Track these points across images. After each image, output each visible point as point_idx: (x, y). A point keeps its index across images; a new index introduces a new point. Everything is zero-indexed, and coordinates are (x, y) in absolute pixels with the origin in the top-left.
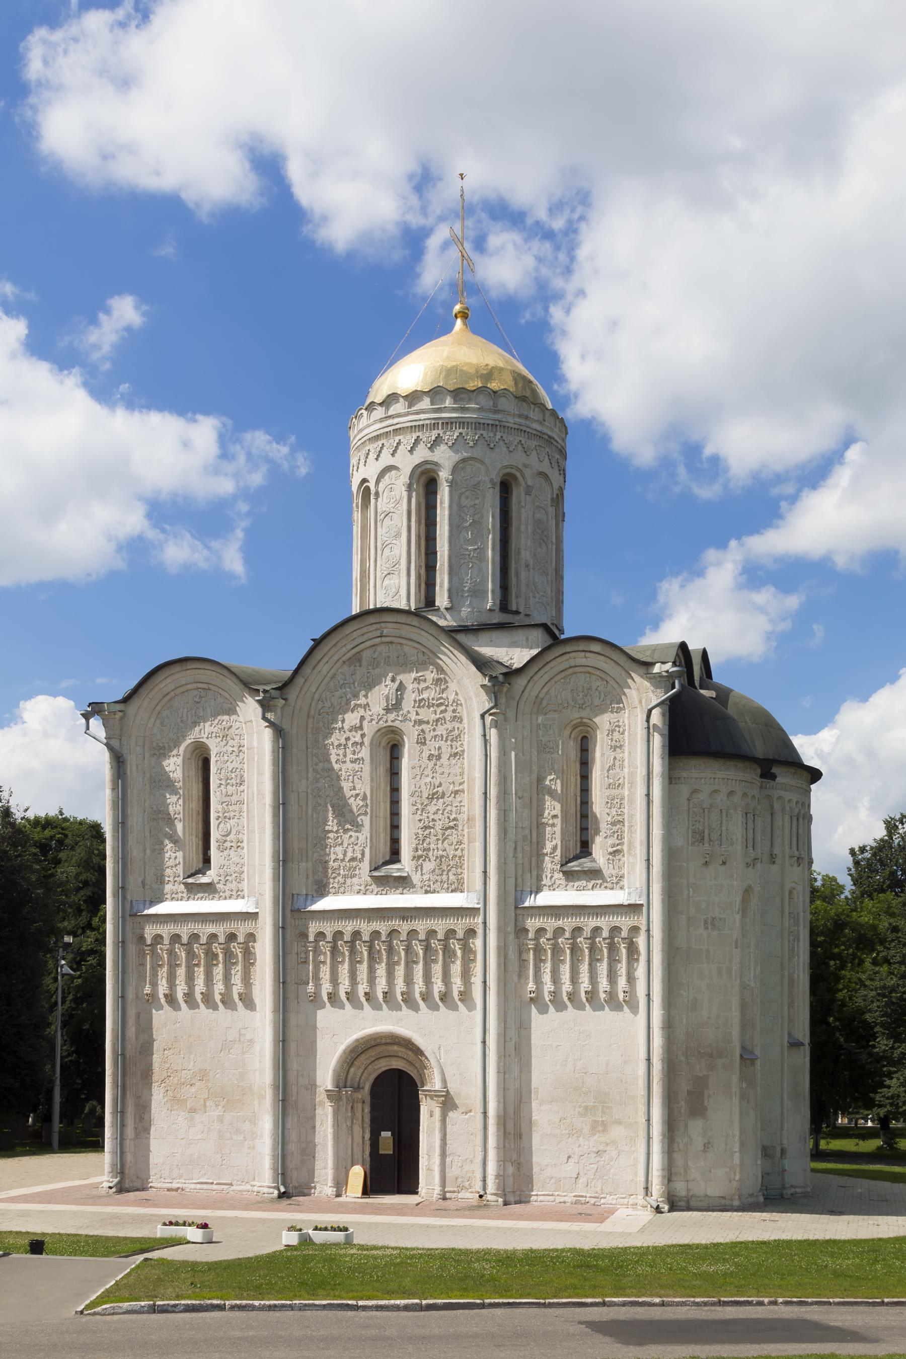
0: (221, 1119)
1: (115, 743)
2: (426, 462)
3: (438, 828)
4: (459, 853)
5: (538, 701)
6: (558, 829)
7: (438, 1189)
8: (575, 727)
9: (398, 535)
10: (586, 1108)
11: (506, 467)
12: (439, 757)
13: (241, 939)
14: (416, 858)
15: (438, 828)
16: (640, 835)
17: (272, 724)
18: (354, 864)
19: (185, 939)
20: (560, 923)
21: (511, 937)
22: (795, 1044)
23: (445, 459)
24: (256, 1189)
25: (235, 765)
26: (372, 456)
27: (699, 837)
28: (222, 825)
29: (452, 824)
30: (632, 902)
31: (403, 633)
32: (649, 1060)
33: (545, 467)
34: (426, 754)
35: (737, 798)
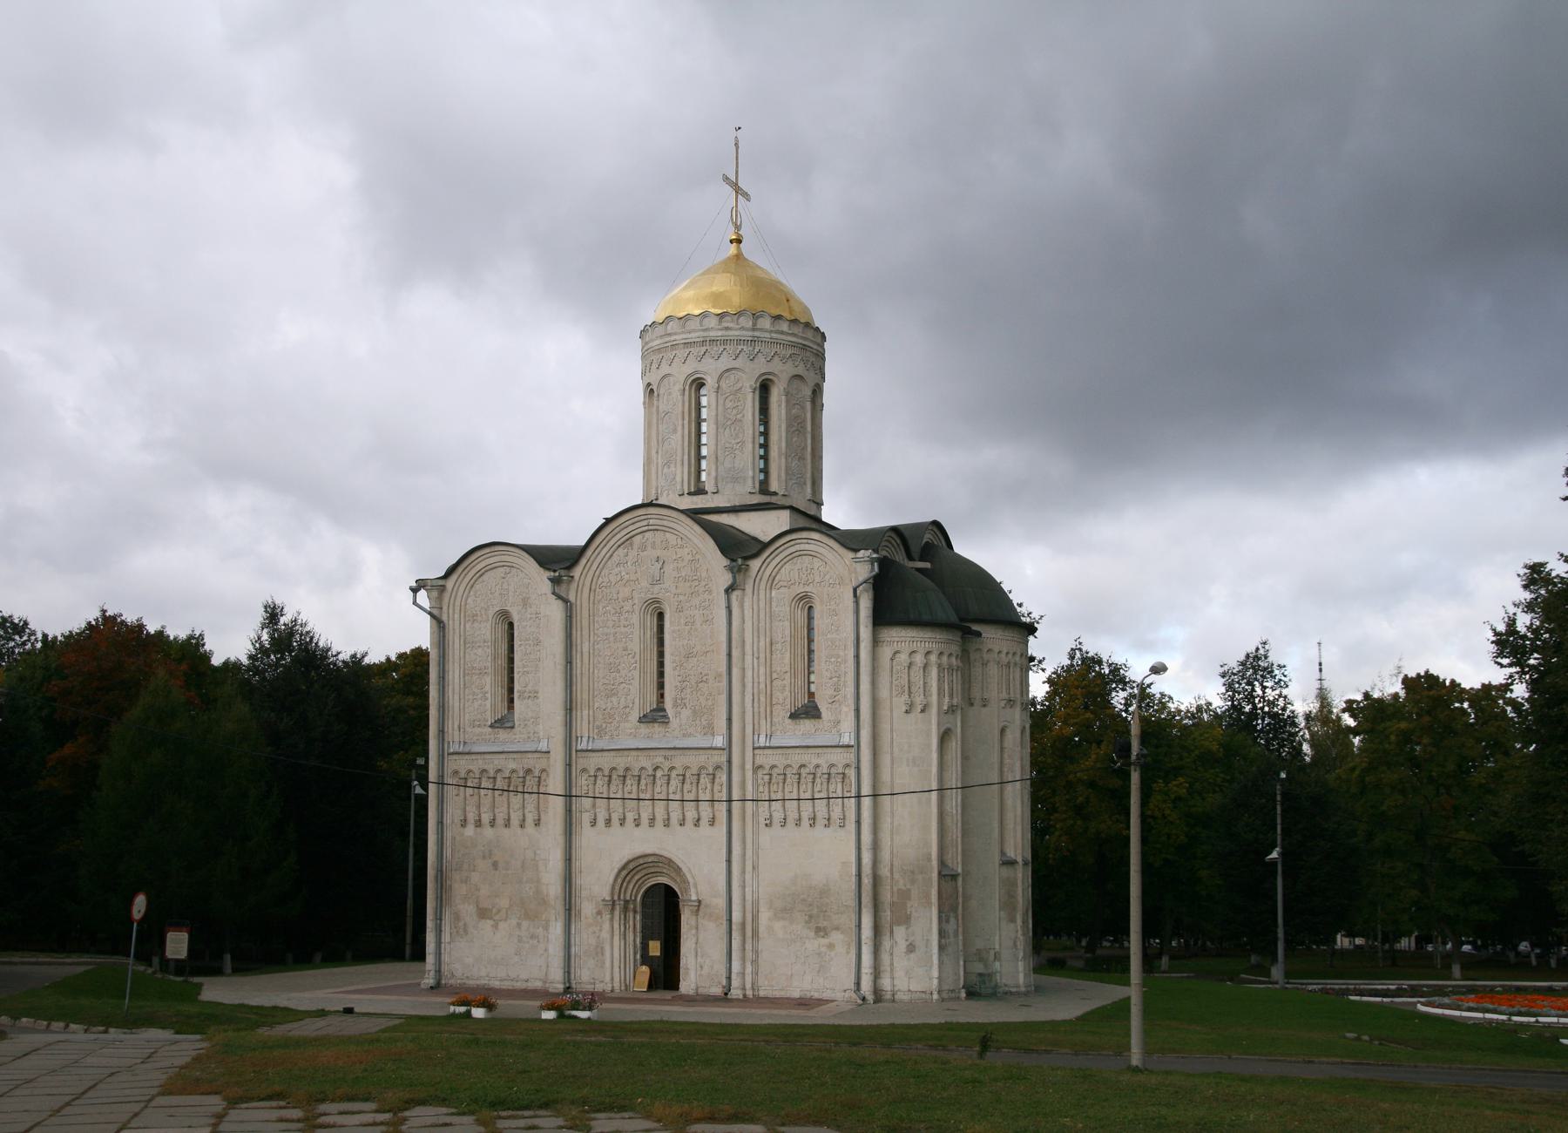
0: (519, 925)
1: (435, 612)
6: (787, 682)
7: (693, 986)
8: (801, 599)
9: (675, 431)
14: (675, 705)
16: (851, 690)
17: (559, 597)
21: (749, 774)
22: (1011, 863)
23: (710, 369)
26: (654, 366)
32: (859, 875)
33: (800, 370)
35: (933, 658)
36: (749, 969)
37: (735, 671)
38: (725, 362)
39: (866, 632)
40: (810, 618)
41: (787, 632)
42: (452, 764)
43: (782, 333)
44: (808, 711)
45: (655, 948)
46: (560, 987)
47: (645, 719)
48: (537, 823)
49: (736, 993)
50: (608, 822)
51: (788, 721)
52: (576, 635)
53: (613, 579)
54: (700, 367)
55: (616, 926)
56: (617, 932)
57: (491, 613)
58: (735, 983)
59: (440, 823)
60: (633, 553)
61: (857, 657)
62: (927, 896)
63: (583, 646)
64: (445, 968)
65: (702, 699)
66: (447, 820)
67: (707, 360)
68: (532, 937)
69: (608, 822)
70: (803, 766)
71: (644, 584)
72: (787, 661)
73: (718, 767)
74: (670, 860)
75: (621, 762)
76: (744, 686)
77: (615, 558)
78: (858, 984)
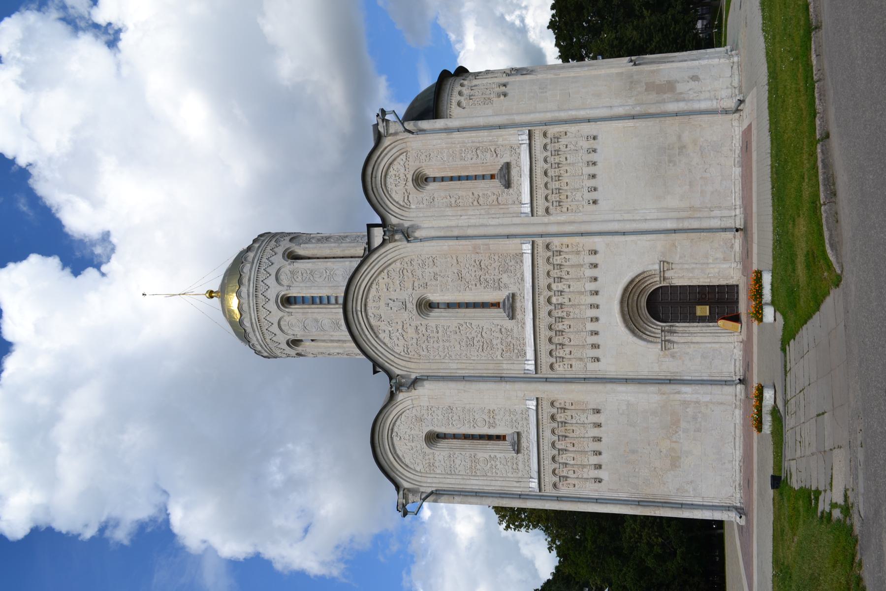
2: (277, 302)
3: (481, 273)
4: (496, 258)
5: (401, 207)
9: (317, 321)
10: (670, 161)
11: (283, 257)
12: (435, 274)
13: (554, 411)
15: (481, 273)
18: (503, 330)
19: (555, 452)
20: (542, 186)
21: (552, 218)
23: (274, 291)
24: (738, 403)
25: (440, 414)
27: (487, 101)
28: (479, 424)
29: (478, 263)
30: (527, 137)
31: (360, 297)
34: (434, 283)
36: (717, 213)
37: (470, 232)
38: (271, 281)
39: (439, 123)
40: (435, 179)
41: (443, 194)
42: (549, 490)
43: (259, 247)
44: (505, 176)
45: (703, 310)
46: (740, 387)
47: (512, 316)
48: (598, 411)
49: (739, 224)
50: (595, 346)
51: (511, 190)
52: (442, 373)
53: (402, 342)
54: (273, 300)
55: (682, 340)
56: (689, 339)
57: (427, 450)
58: (729, 223)
59: (597, 501)
60: (383, 326)
61: (459, 130)
62: (653, 72)
63: (453, 367)
64: (728, 502)
65: (494, 265)
66: (595, 495)
67: (268, 294)
68: (695, 418)
69: (595, 346)
70: (546, 173)
71: (405, 315)
72: (464, 194)
73: (547, 247)
74: (625, 290)
75: (544, 333)
76: (482, 225)
77: (387, 340)
78: (726, 112)
